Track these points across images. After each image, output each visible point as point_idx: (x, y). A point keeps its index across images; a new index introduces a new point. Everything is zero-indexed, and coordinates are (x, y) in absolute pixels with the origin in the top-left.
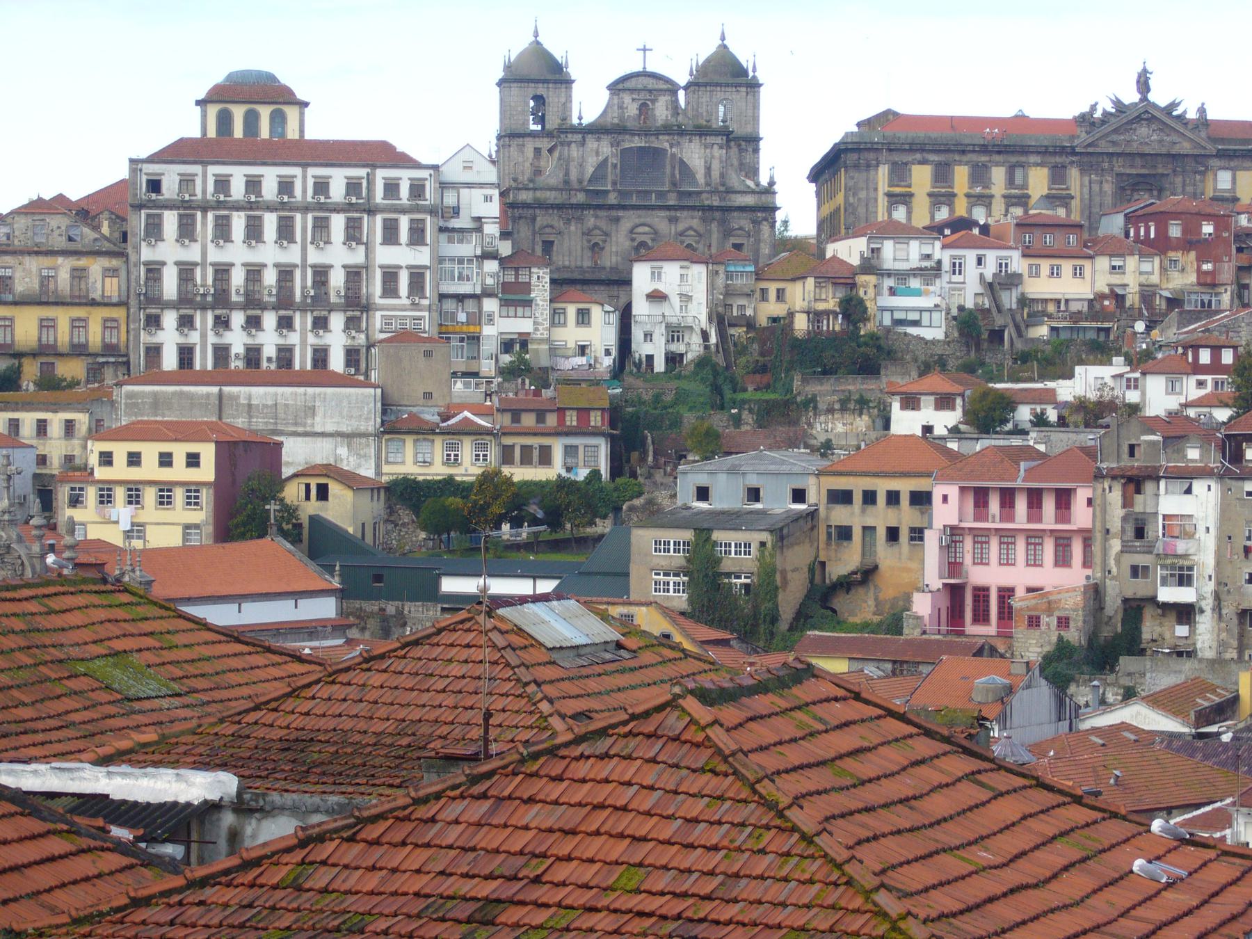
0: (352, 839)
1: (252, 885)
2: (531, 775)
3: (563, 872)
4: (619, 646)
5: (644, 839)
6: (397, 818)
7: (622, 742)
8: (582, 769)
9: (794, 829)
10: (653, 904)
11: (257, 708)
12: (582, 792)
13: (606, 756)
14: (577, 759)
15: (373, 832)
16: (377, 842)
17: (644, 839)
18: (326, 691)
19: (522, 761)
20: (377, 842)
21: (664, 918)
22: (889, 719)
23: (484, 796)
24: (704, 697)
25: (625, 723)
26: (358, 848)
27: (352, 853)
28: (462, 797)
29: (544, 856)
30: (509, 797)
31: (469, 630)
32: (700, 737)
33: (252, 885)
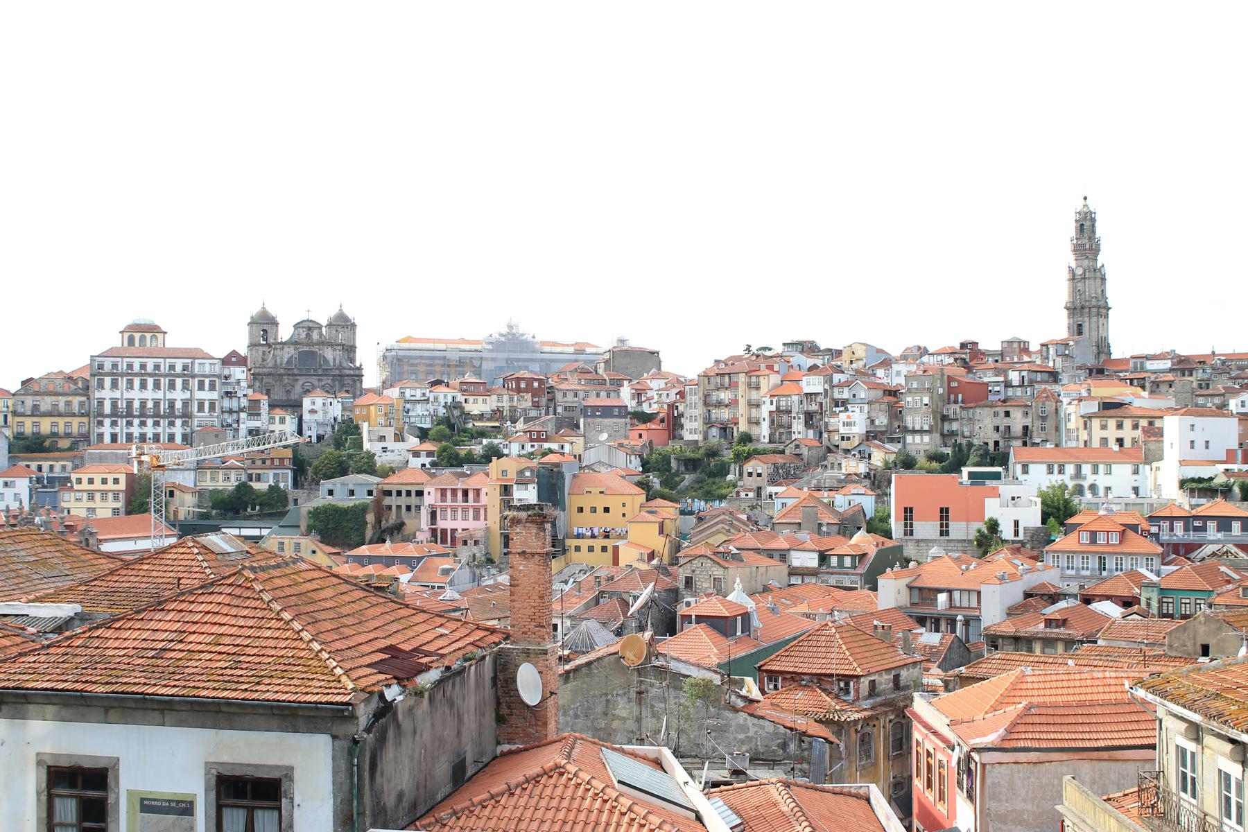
0: (109, 628)
1: (68, 646)
2: (182, 601)
3: (192, 638)
4: (248, 552)
5: (224, 625)
6: (128, 619)
7: (218, 588)
8: (202, 599)
9: (282, 619)
10: (225, 649)
11: (96, 579)
12: (202, 607)
13: (212, 593)
14: (200, 594)
15: (118, 625)
16: (119, 628)
17: (224, 625)
18: (124, 572)
19: (178, 596)
20: (119, 628)
21: (229, 654)
22: (332, 578)
23: (163, 610)
24: (253, 569)
25: (220, 580)
26: (111, 631)
27: (109, 634)
28: (154, 610)
29: (185, 632)
30: (173, 610)
31: (184, 547)
32: (249, 585)
33: (68, 646)
